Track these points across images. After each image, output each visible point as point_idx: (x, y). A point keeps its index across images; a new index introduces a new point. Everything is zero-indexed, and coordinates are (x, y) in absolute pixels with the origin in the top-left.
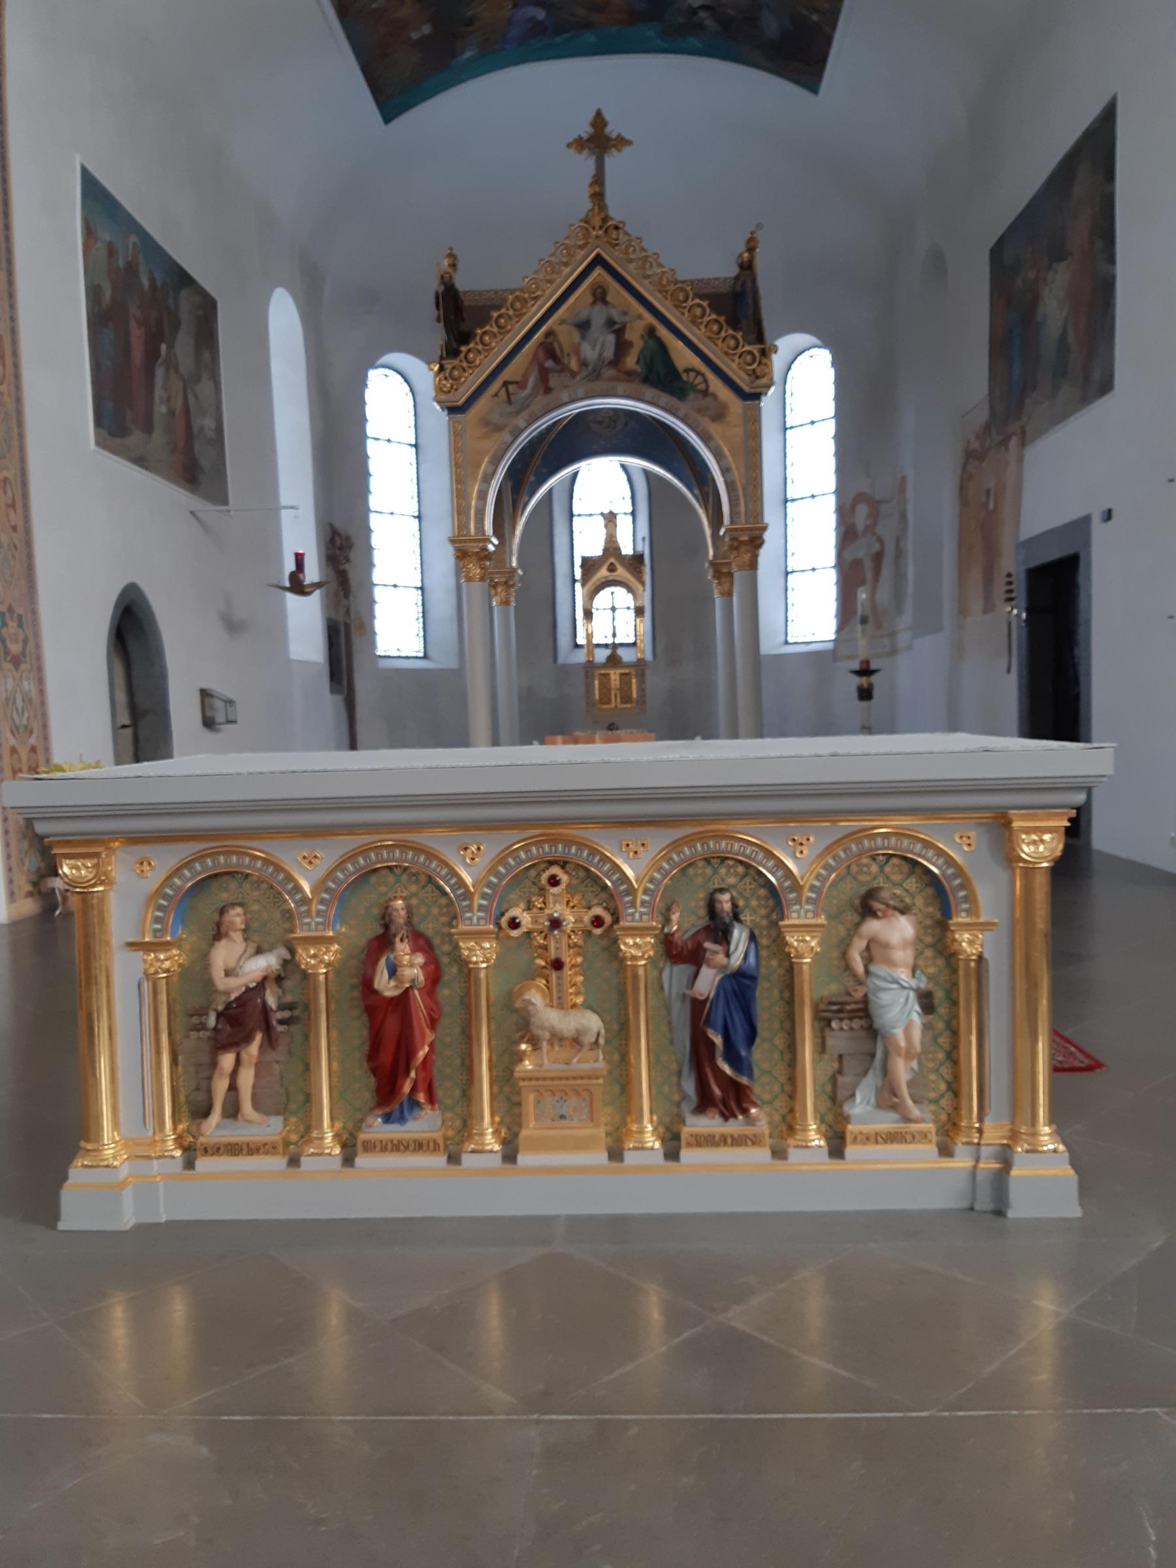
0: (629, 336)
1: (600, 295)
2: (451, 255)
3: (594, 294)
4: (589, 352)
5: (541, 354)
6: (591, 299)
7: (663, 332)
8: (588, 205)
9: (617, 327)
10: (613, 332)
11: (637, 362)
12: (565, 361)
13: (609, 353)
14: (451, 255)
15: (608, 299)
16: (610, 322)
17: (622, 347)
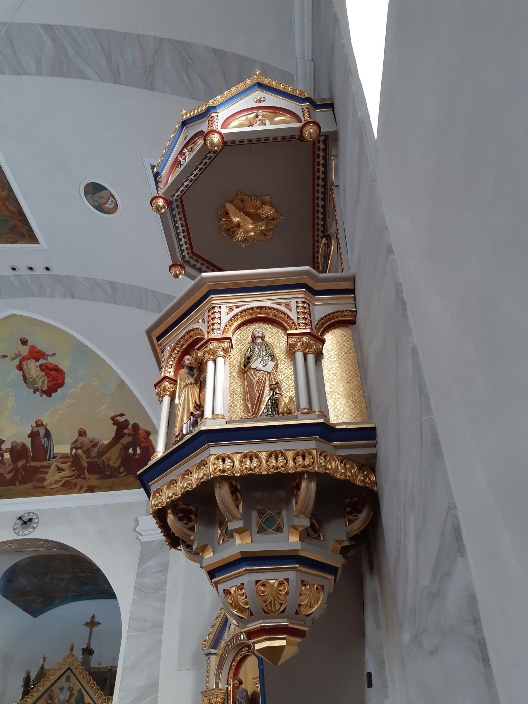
0: (74, 692)
1: (68, 679)
2: (44, 658)
3: (67, 678)
4: (61, 697)
5: (48, 698)
6: (65, 680)
7: (83, 691)
8: (69, 651)
9: (71, 689)
10: (70, 691)
11: (74, 701)
12: (54, 700)
13: (67, 698)
14: (44, 658)
15: (70, 680)
16: (70, 688)
17: (71, 696)
